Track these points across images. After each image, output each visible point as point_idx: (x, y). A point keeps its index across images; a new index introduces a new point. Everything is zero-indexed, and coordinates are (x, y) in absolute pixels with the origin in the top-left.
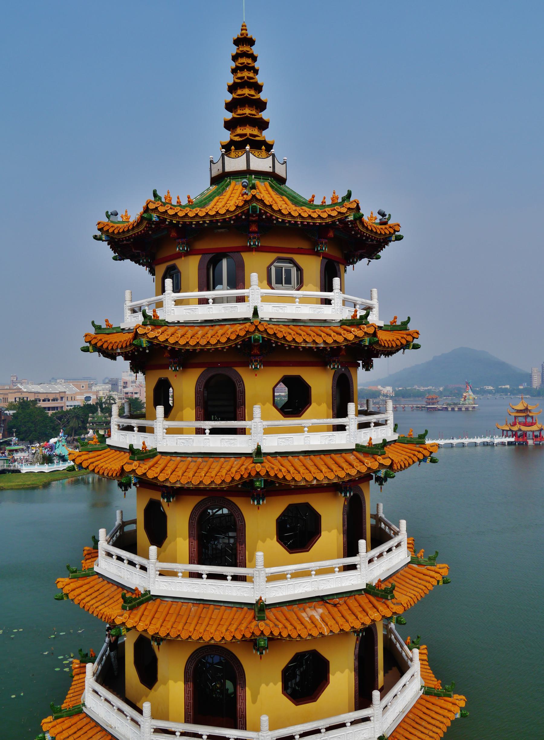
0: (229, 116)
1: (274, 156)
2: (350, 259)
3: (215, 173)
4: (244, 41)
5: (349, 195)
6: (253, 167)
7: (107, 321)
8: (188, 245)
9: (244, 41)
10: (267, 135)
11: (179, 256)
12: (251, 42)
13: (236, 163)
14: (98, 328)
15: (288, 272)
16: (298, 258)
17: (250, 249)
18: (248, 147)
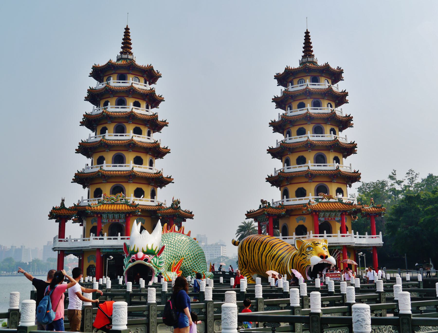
3: (119, 58)
4: (127, 29)
9: (127, 29)
11: (112, 74)
12: (129, 29)
13: (124, 56)
16: (139, 77)
17: (129, 73)
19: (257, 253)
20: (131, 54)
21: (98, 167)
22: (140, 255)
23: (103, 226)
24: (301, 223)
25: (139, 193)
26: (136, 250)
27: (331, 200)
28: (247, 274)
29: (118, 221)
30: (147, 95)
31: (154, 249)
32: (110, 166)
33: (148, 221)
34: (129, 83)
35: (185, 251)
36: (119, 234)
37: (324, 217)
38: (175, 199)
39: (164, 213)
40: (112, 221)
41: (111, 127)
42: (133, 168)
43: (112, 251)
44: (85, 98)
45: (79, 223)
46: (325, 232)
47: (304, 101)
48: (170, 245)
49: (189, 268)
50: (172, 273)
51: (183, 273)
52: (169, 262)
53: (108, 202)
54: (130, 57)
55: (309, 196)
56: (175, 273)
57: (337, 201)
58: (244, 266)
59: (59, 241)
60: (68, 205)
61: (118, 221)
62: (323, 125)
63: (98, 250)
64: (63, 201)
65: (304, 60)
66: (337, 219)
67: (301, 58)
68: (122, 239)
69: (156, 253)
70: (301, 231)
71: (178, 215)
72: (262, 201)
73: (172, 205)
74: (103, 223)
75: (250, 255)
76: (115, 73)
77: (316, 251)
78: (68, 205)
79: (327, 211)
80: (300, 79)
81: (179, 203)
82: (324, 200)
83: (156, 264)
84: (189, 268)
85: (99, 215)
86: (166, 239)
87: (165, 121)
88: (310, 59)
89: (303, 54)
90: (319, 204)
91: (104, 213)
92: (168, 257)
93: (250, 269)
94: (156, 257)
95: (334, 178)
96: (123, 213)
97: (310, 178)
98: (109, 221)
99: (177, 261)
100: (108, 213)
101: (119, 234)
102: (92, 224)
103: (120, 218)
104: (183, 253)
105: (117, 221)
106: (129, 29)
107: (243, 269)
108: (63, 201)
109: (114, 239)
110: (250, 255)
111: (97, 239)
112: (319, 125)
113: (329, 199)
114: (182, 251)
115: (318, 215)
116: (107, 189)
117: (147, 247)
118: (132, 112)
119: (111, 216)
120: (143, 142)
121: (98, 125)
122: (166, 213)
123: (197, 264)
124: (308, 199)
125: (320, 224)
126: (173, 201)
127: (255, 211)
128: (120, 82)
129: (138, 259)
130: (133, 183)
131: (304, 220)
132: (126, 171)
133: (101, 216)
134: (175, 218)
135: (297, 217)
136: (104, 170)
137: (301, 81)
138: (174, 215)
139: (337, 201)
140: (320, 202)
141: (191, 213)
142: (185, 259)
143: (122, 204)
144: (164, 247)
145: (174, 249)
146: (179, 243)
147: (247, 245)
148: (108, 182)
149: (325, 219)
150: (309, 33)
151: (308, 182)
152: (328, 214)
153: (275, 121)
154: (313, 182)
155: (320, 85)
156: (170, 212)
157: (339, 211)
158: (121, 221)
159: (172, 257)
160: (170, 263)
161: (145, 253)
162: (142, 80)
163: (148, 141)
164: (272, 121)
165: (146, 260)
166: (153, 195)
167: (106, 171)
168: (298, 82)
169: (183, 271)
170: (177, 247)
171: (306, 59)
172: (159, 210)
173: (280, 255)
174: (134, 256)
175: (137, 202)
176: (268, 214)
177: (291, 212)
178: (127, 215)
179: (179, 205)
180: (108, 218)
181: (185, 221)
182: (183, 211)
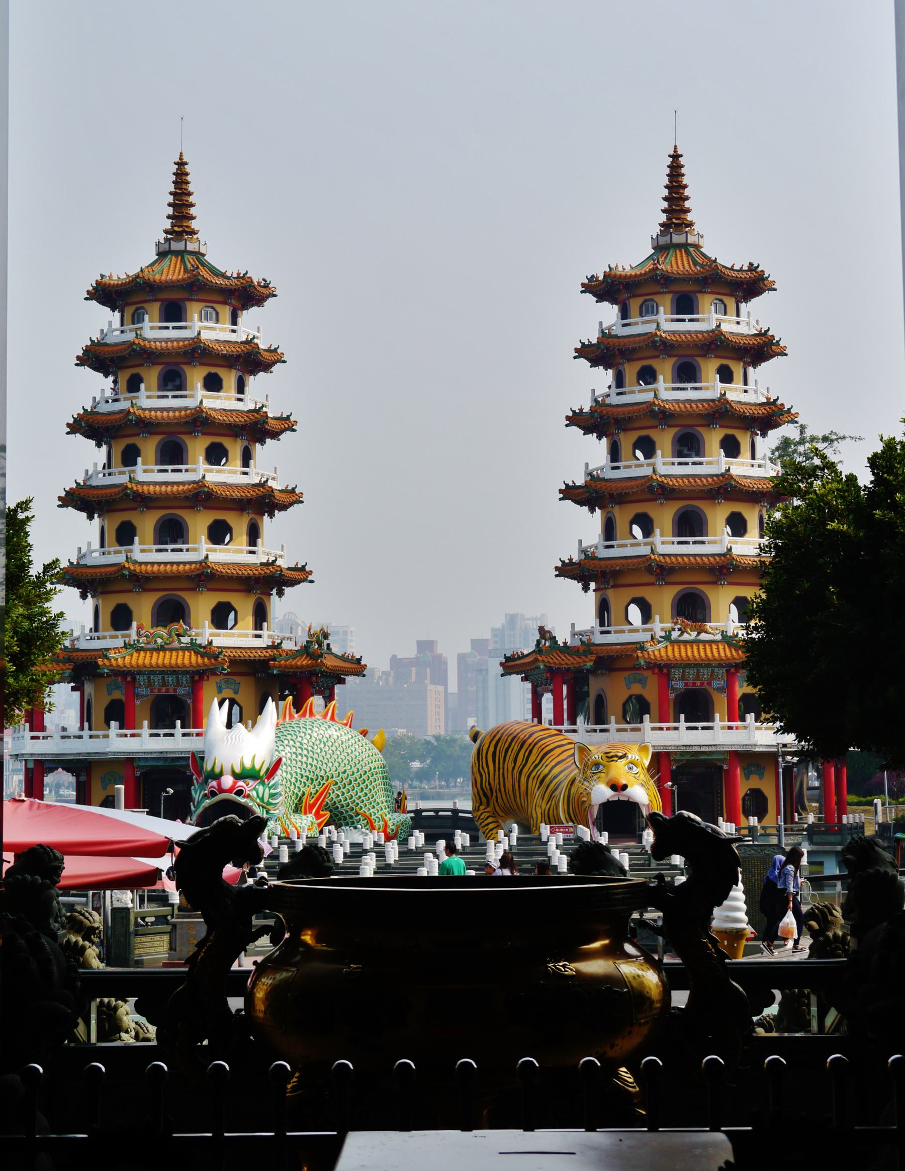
2: (245, 307)
5: (247, 273)
6: (189, 248)
9: (181, 164)
13: (176, 246)
15: (211, 314)
16: (216, 306)
17: (191, 300)
19: (510, 769)
21: (120, 552)
22: (228, 781)
23: (138, 702)
24: (637, 689)
26: (217, 770)
27: (703, 637)
28: (490, 820)
29: (175, 690)
30: (239, 356)
31: (257, 767)
32: (150, 551)
33: (246, 696)
34: (190, 328)
35: (337, 764)
36: (178, 723)
37: (683, 678)
38: (316, 629)
39: (286, 666)
40: (159, 690)
43: (161, 763)
44: (78, 358)
45: (69, 683)
46: (682, 716)
47: (655, 364)
48: (299, 751)
49: (348, 805)
50: (304, 817)
51: (331, 817)
52: (296, 791)
53: (149, 646)
54: (191, 247)
55: (654, 622)
56: (311, 817)
57: (719, 637)
58: (483, 799)
59: (32, 738)
62: (699, 429)
63: (129, 762)
65: (663, 240)
66: (715, 684)
67: (657, 229)
68: (184, 735)
69: (262, 773)
70: (637, 709)
71: (322, 673)
72: (541, 630)
74: (140, 696)
75: (497, 772)
77: (607, 774)
79: (689, 666)
80: (645, 301)
81: (326, 636)
82: (686, 637)
83: (262, 799)
84: (348, 805)
85: (129, 679)
86: (289, 737)
87: (288, 417)
88: (677, 239)
89: (663, 218)
90: (670, 648)
91: (140, 673)
92: (293, 780)
93: (497, 808)
94: (263, 783)
95: (722, 574)
96: (187, 672)
97: (658, 574)
98: (152, 691)
99: (317, 788)
100: (150, 672)
101: (178, 723)
102: (110, 693)
103: (178, 684)
104: (330, 769)
105: (171, 692)
107: (482, 807)
109: (165, 735)
110: (497, 772)
111: (126, 736)
112: (690, 430)
113: (699, 634)
114: (330, 765)
115: (668, 674)
116: (143, 608)
117: (242, 764)
119: (156, 680)
120: (231, 486)
122: (291, 667)
123: (366, 794)
124: (651, 630)
125: (672, 696)
126: (310, 635)
127: (524, 656)
128: (167, 328)
129: (222, 791)
131: (642, 681)
132: (190, 563)
133: (134, 679)
134: (314, 679)
135: (626, 674)
137: (650, 304)
138: (313, 673)
139: (719, 637)
140: (673, 642)
141: (359, 660)
142: (337, 783)
143: (183, 649)
144: (280, 760)
145: (310, 760)
146: (322, 746)
147: (492, 749)
148: (145, 590)
149: (686, 684)
150: (681, 156)
151: (653, 584)
152: (691, 673)
153: (581, 410)
154: (668, 583)
155: (697, 320)
156: (302, 666)
157: (720, 666)
158: (181, 691)
159: (304, 780)
160: (300, 794)
161: (237, 777)
162: (225, 312)
163: (244, 480)
164: (574, 412)
165: (240, 793)
166: (261, 616)
167: (141, 564)
168: (641, 307)
169: (331, 811)
170: (316, 756)
171: (667, 238)
172: (274, 659)
173: (555, 778)
174: (214, 783)
175: (218, 642)
176: (549, 669)
177: (612, 661)
178: (197, 678)
179: (326, 642)
180: (149, 684)
181: (343, 682)
182: (336, 656)
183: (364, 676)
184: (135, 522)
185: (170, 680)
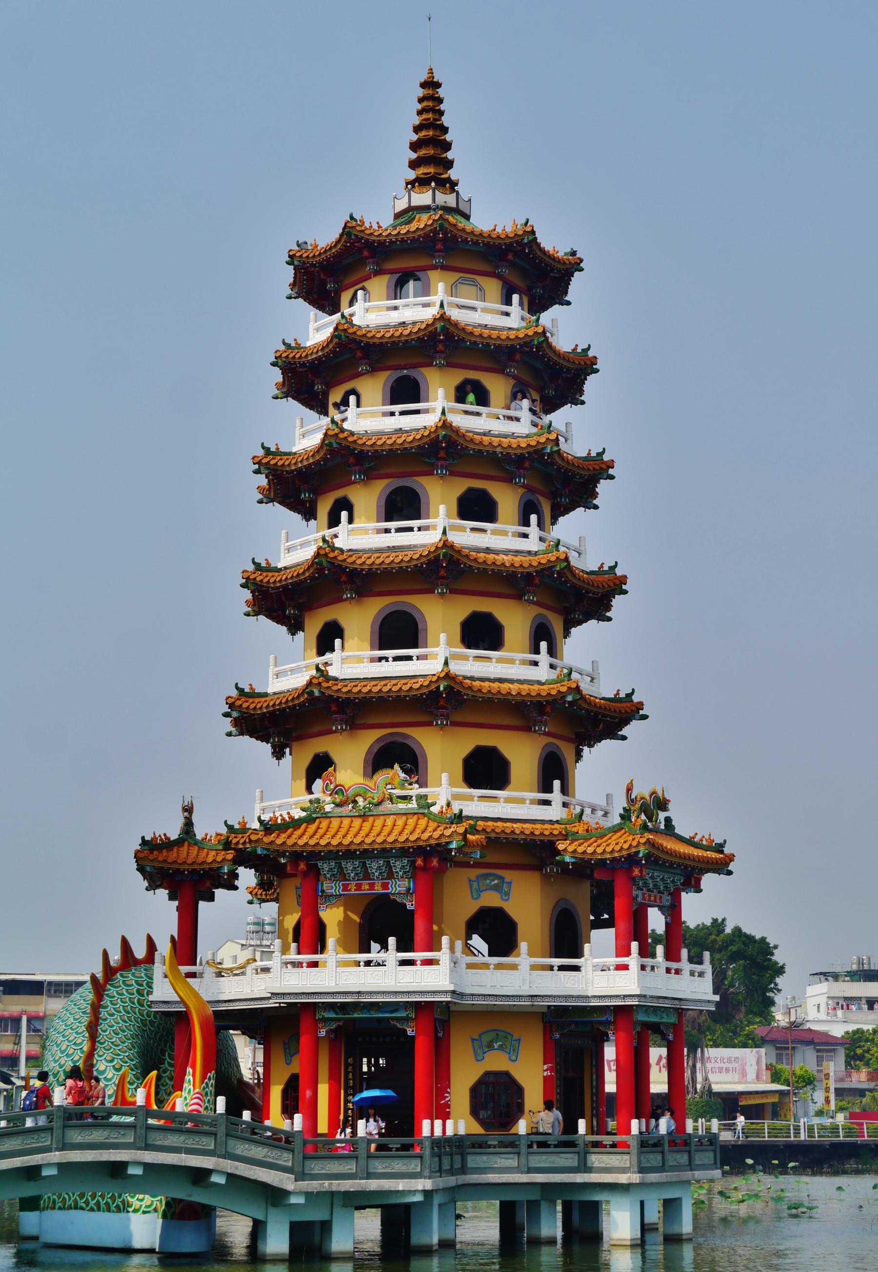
0: (414, 156)
1: (458, 193)
4: (431, 84)
7: (295, 340)
8: (377, 264)
9: (431, 84)
10: (453, 174)
12: (438, 85)
13: (422, 198)
14: (288, 346)
17: (434, 267)
18: (433, 184)
20: (451, 185)
25: (486, 770)
29: (385, 886)
38: (642, 790)
40: (359, 887)
41: (367, 498)
42: (446, 663)
60: (208, 827)
61: (385, 886)
64: (188, 810)
68: (404, 963)
73: (625, 816)
76: (378, 273)
78: (208, 827)
81: (662, 804)
98: (345, 888)
103: (391, 875)
105: (378, 889)
106: (438, 85)
108: (188, 810)
116: (349, 756)
118: (446, 425)
121: (319, 491)
126: (631, 801)
130: (454, 724)
134: (636, 872)
136: (336, 679)
138: (632, 859)
162: (493, 287)
166: (553, 772)
172: (565, 837)
178: (419, 862)
183: (730, 873)
184: (344, 623)
185: (374, 866)
